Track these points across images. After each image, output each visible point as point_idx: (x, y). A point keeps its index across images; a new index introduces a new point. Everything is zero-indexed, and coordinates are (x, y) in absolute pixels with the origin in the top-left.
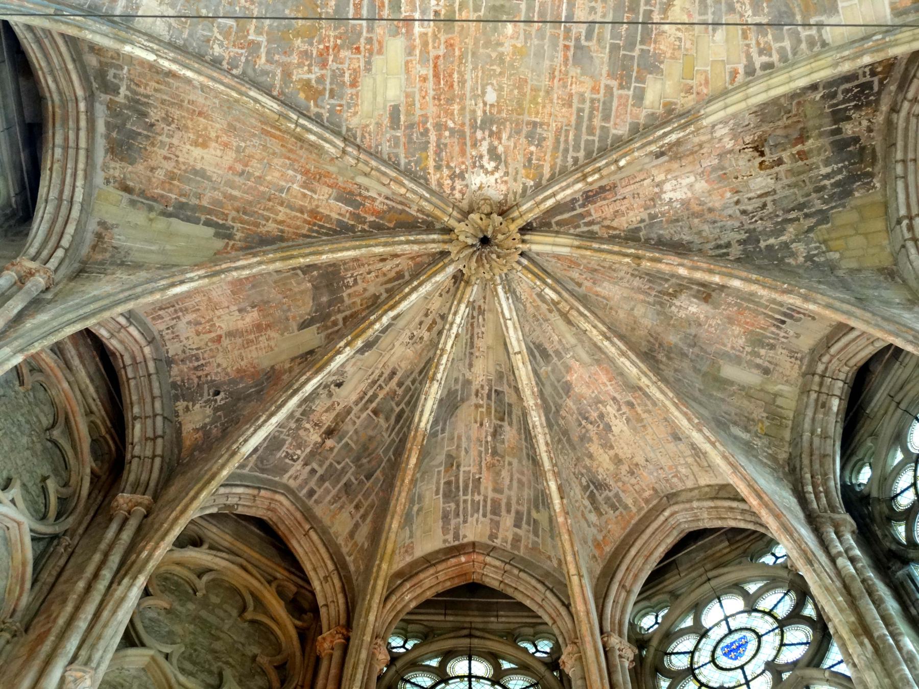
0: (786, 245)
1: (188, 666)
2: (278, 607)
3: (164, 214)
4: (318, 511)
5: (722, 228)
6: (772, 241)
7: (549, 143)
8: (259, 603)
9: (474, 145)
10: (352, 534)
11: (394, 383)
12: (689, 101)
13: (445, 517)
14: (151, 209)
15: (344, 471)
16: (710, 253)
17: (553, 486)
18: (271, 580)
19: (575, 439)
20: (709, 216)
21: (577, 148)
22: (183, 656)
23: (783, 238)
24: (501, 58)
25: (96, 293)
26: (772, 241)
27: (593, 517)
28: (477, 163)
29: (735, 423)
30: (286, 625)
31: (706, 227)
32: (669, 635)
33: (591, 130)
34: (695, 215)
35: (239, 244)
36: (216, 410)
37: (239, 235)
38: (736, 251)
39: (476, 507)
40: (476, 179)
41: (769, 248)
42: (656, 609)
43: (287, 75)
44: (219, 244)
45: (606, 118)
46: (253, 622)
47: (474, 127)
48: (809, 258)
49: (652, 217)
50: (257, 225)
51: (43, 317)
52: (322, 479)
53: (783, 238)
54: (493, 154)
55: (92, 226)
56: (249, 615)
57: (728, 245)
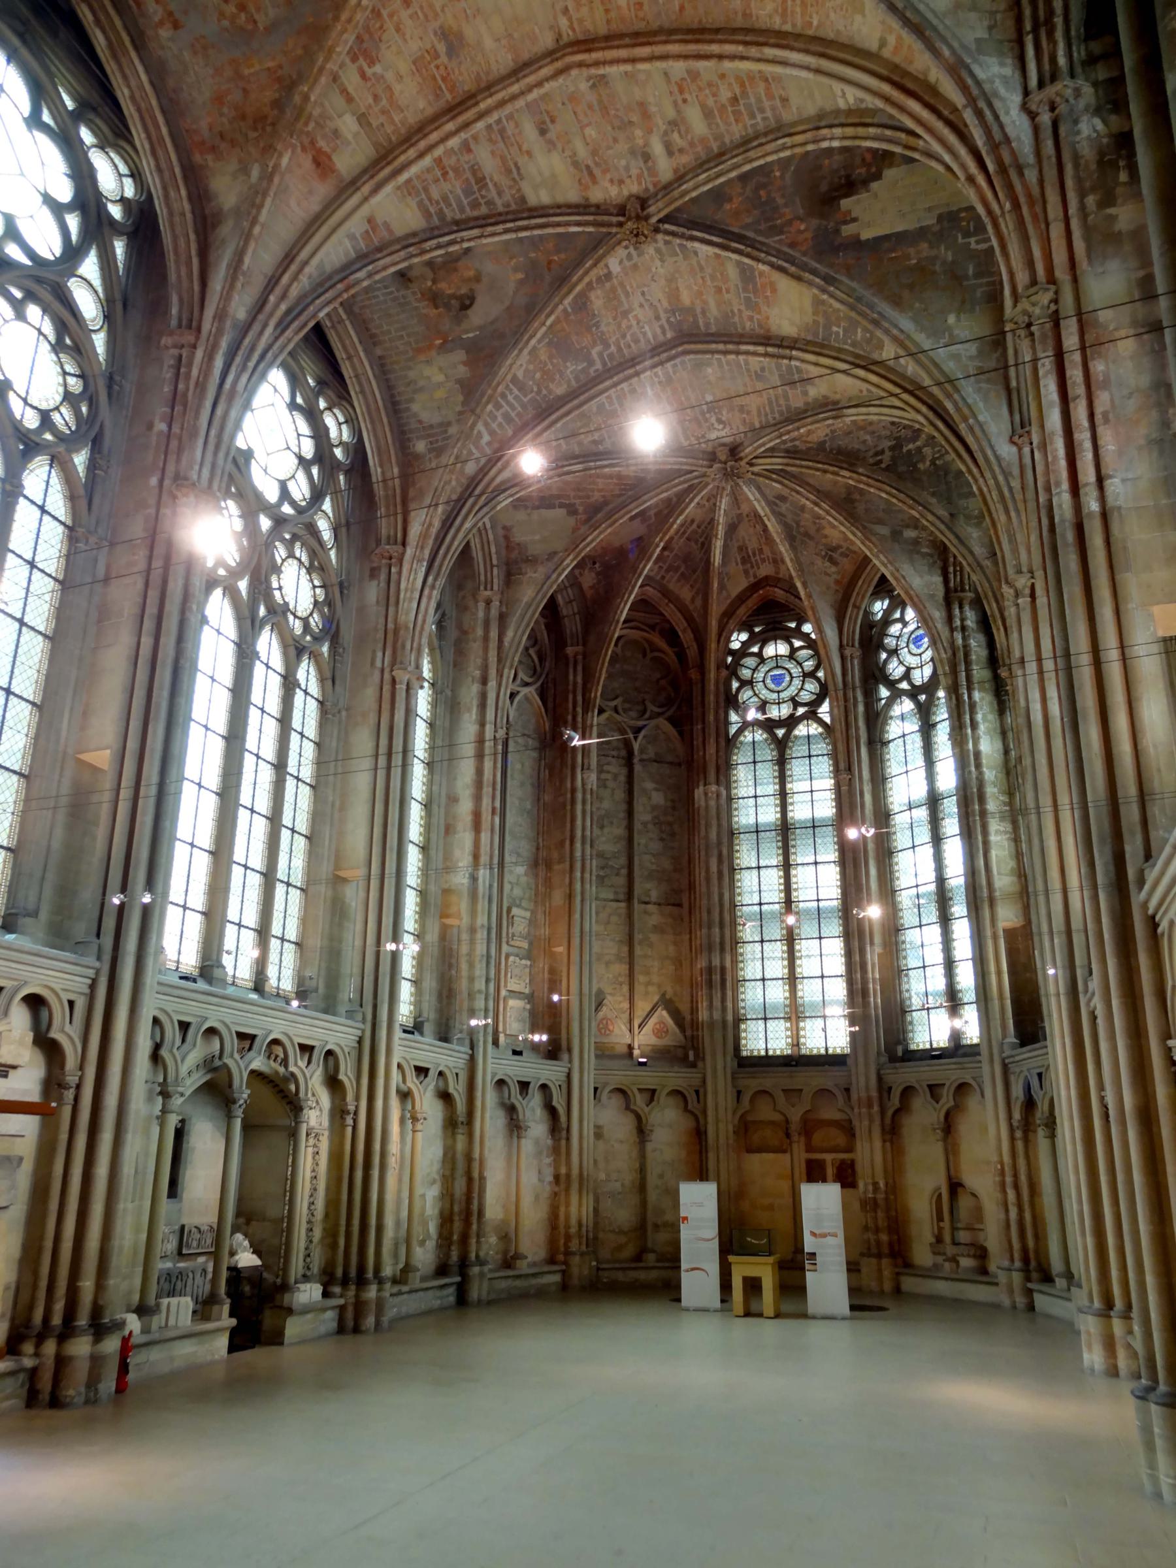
0: (919, 449)
1: (627, 706)
2: (661, 643)
3: (538, 508)
4: (671, 586)
5: (879, 437)
6: (911, 446)
7: (755, 413)
8: (654, 648)
9: (706, 420)
10: (693, 600)
11: (694, 526)
12: (838, 397)
13: (746, 572)
14: (526, 507)
15: (678, 568)
16: (871, 461)
17: (799, 585)
18: (653, 627)
19: (812, 532)
20: (870, 428)
21: (772, 412)
22: (624, 701)
23: (918, 443)
24: (709, 382)
25: (525, 599)
26: (911, 446)
27: (834, 569)
28: (711, 428)
29: (908, 526)
30: (670, 655)
31: (868, 437)
32: (887, 621)
33: (779, 406)
34: (863, 428)
35: (584, 517)
36: (598, 574)
37: (581, 509)
38: (887, 457)
39: (763, 561)
40: (713, 435)
41: (909, 451)
42: (883, 600)
43: (580, 444)
44: (571, 521)
45: (787, 399)
46: (654, 659)
47: (703, 414)
48: (933, 462)
49: (833, 432)
50: (588, 497)
51: (510, 634)
52: (667, 571)
53: (918, 443)
54: (719, 421)
55: (501, 532)
56: (649, 655)
57: (882, 452)
